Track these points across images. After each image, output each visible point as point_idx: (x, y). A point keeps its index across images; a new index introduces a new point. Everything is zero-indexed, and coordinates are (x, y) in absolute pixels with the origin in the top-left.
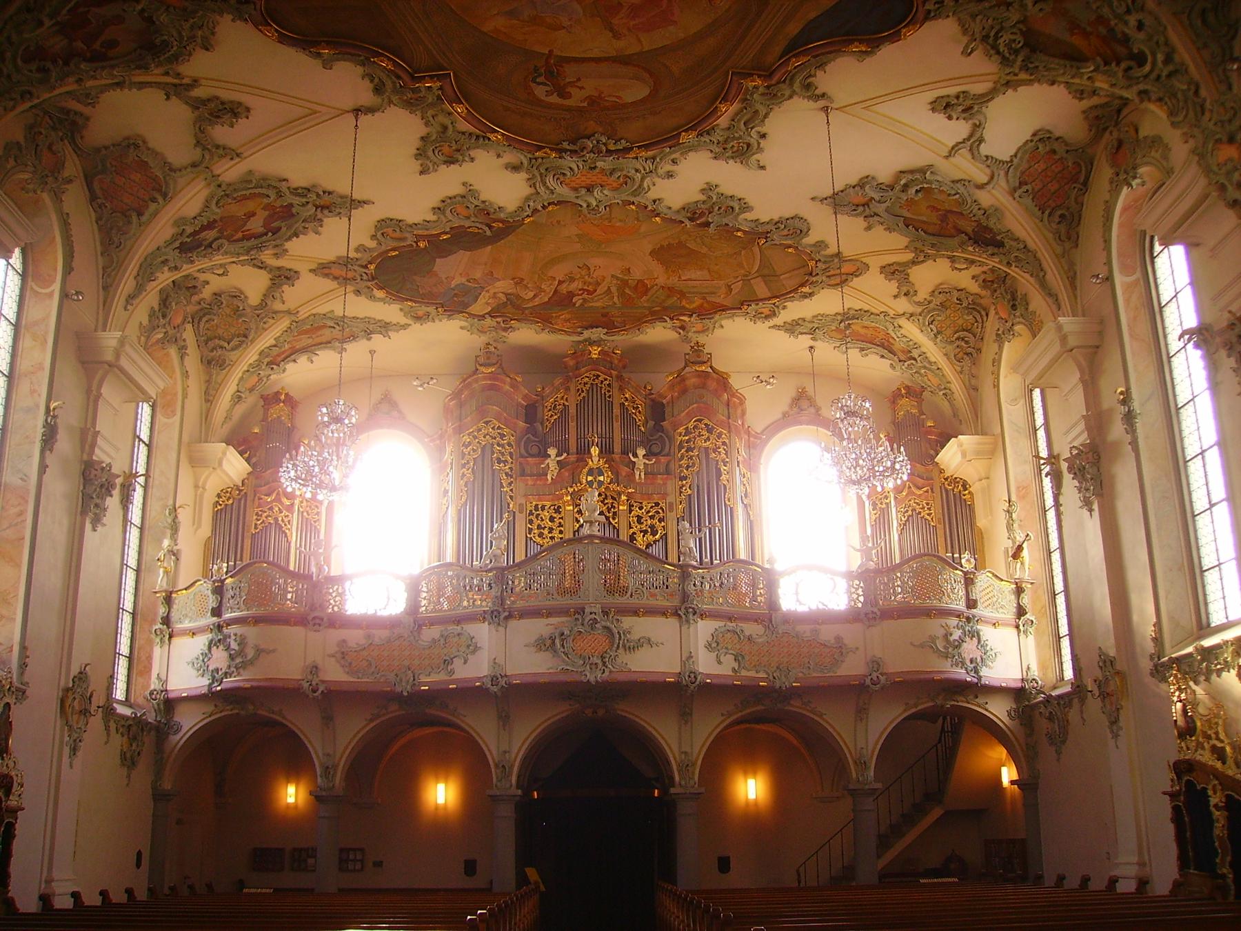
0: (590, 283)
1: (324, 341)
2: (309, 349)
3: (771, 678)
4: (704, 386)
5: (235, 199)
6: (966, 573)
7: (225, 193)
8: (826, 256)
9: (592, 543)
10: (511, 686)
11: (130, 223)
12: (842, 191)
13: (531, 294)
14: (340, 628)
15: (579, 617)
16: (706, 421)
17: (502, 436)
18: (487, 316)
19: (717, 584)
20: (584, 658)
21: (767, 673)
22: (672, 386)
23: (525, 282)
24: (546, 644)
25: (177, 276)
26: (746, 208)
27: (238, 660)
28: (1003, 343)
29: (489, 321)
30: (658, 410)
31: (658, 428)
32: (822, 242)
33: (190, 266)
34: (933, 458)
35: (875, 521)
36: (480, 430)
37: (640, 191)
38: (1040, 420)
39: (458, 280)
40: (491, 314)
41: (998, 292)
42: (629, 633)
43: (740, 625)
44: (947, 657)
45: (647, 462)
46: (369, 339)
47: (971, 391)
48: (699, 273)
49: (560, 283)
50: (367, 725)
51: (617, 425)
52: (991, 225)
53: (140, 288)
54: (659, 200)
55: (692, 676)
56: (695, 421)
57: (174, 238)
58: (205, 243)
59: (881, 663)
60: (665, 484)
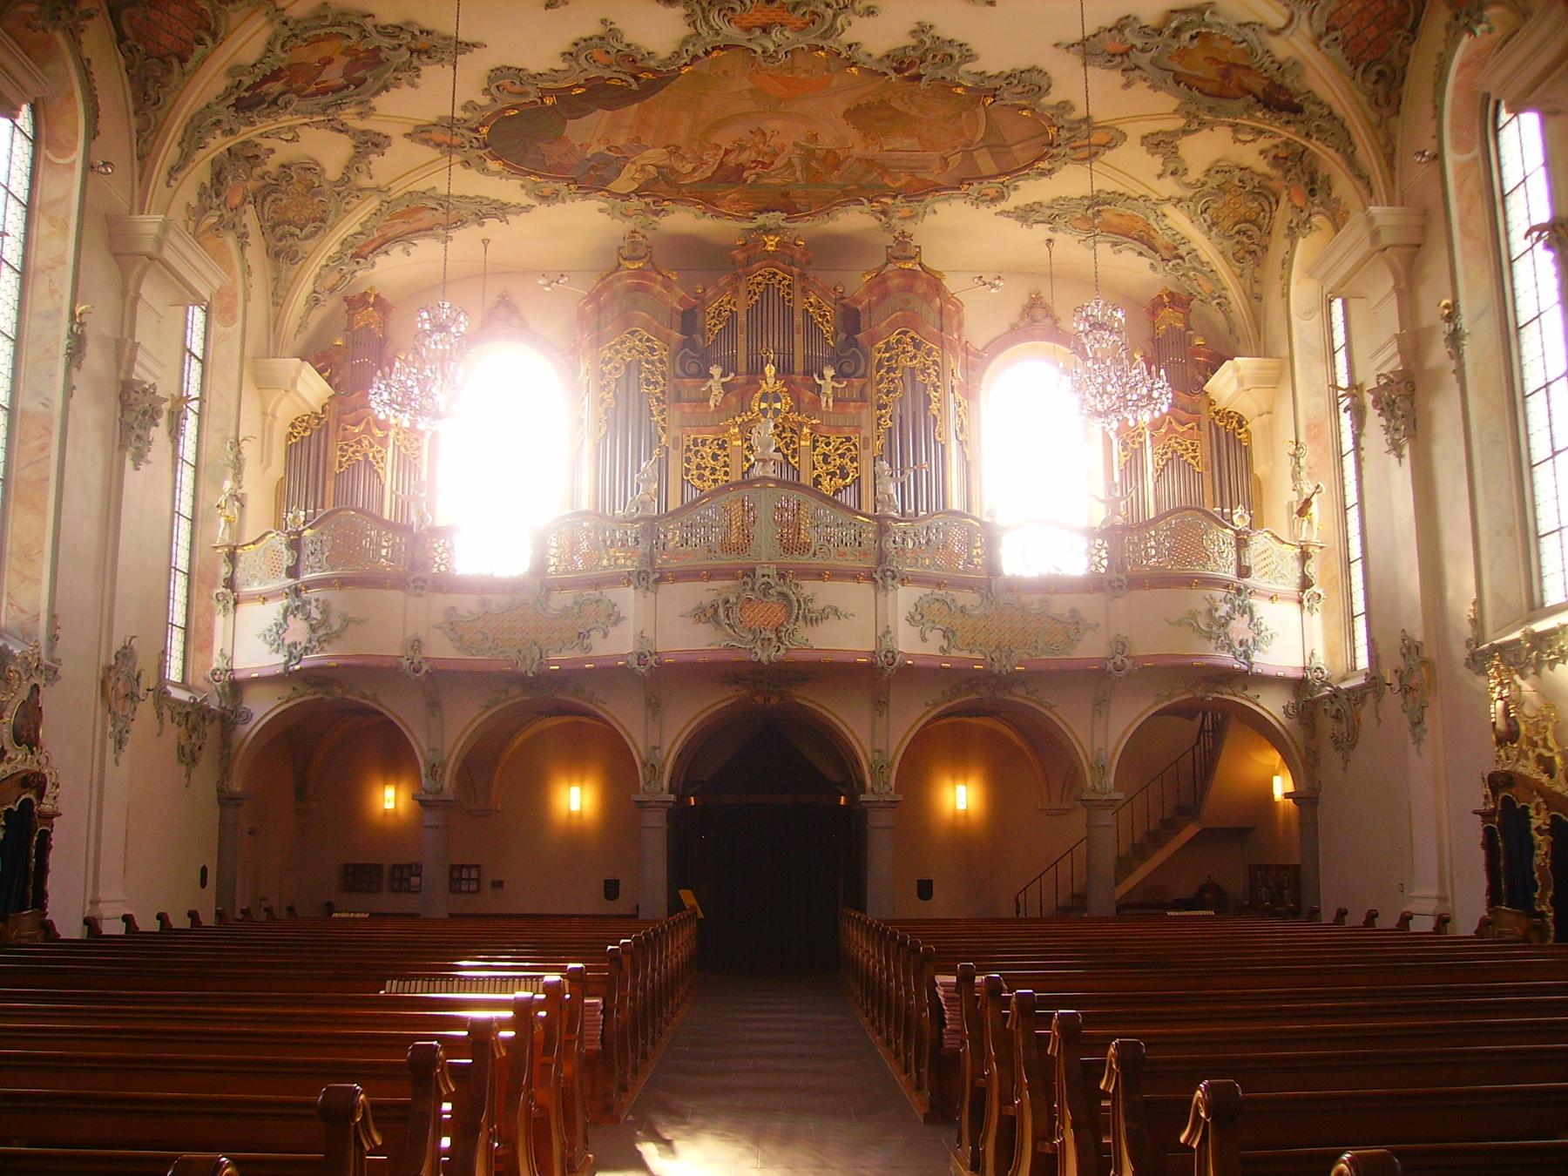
0: (766, 154)
1: (424, 226)
2: (405, 238)
3: (989, 659)
5: (305, 40)
6: (1238, 533)
10: (661, 664)
11: (170, 72)
12: (1094, 36)
13: (689, 167)
14: (447, 592)
15: (749, 580)
17: (652, 350)
18: (632, 195)
19: (923, 541)
22: (869, 288)
24: (707, 614)
25: (232, 141)
26: (969, 56)
27: (321, 632)
28: (1296, 238)
29: (635, 199)
30: (851, 319)
31: (851, 341)
32: (1067, 102)
33: (251, 128)
35: (1125, 464)
37: (830, 32)
38: (1339, 338)
41: (1293, 171)
44: (1210, 638)
45: (836, 385)
47: (1255, 303)
49: (727, 152)
50: (481, 714)
51: (798, 338)
52: (1288, 82)
53: (186, 158)
54: (856, 44)
55: (890, 655)
57: (228, 92)
58: (269, 99)
59: (1126, 644)
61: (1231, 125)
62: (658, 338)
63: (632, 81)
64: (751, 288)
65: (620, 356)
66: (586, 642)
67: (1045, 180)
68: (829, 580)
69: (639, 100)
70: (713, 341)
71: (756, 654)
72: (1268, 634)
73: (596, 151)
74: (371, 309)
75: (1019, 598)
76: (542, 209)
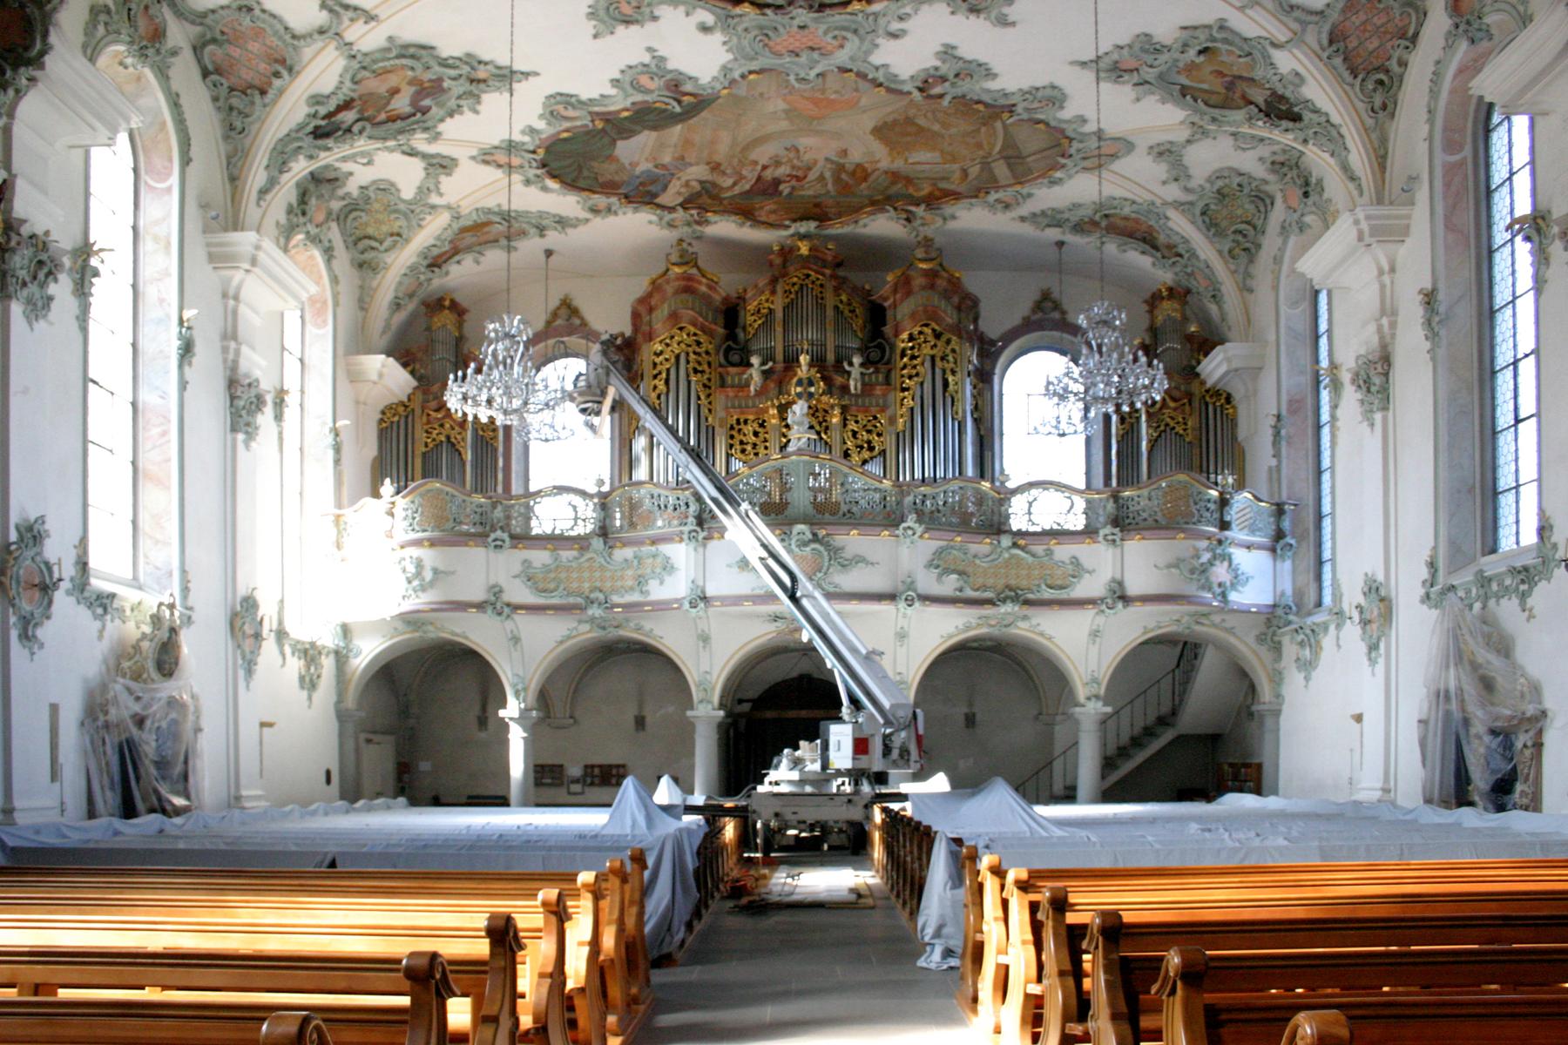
0: (799, 168)
1: (491, 238)
5: (374, 72)
7: (363, 65)
11: (253, 103)
13: (729, 182)
19: (941, 503)
23: (722, 168)
25: (314, 166)
26: (990, 74)
28: (1288, 237)
29: (680, 210)
33: (327, 154)
36: (672, 337)
38: (1323, 327)
40: (685, 205)
41: (1289, 176)
48: (929, 155)
52: (1288, 94)
53: (272, 183)
58: (344, 126)
61: (1234, 134)
63: (675, 104)
69: (681, 121)
72: (1243, 577)
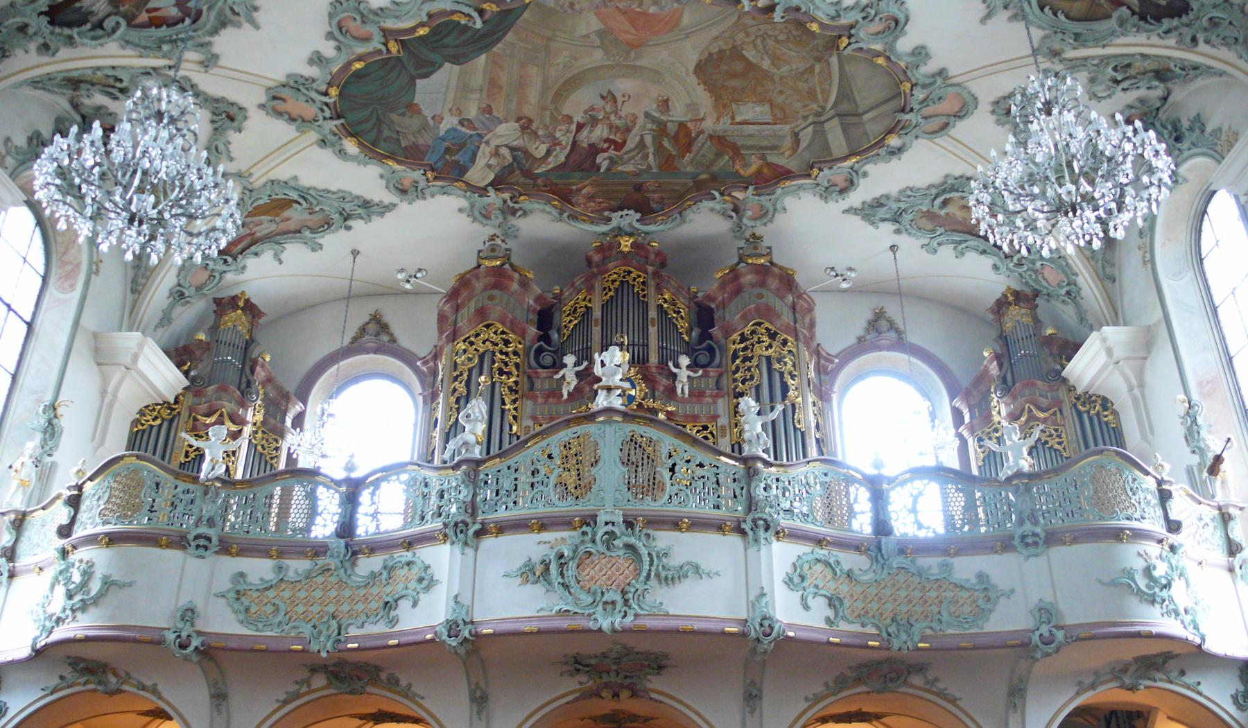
0: (618, 128)
2: (272, 239)
3: (884, 635)
4: (763, 284)
6: (1160, 482)
8: (926, 76)
9: (609, 422)
10: (477, 635)
13: (543, 149)
14: (238, 555)
15: (588, 529)
16: (767, 325)
17: (507, 343)
18: (490, 188)
20: (594, 594)
21: (878, 628)
22: (723, 286)
23: (534, 127)
24: (535, 573)
27: (77, 598)
29: (491, 192)
30: (704, 316)
31: (705, 336)
32: (923, 47)
34: (1058, 373)
35: (983, 460)
36: (477, 335)
39: (450, 122)
40: (497, 184)
42: (666, 555)
43: (835, 553)
44: (1153, 602)
46: (349, 228)
47: (1108, 284)
48: (758, 109)
49: (580, 127)
51: (653, 331)
55: (766, 623)
56: (753, 325)
59: (1054, 612)
60: (715, 403)
62: (514, 332)
63: (475, 15)
64: (606, 285)
65: (474, 347)
66: (393, 613)
67: (894, 161)
68: (688, 530)
69: (487, 48)
70: (569, 336)
71: (596, 620)
73: (449, 126)
74: (240, 312)
75: (913, 561)
76: (404, 207)
